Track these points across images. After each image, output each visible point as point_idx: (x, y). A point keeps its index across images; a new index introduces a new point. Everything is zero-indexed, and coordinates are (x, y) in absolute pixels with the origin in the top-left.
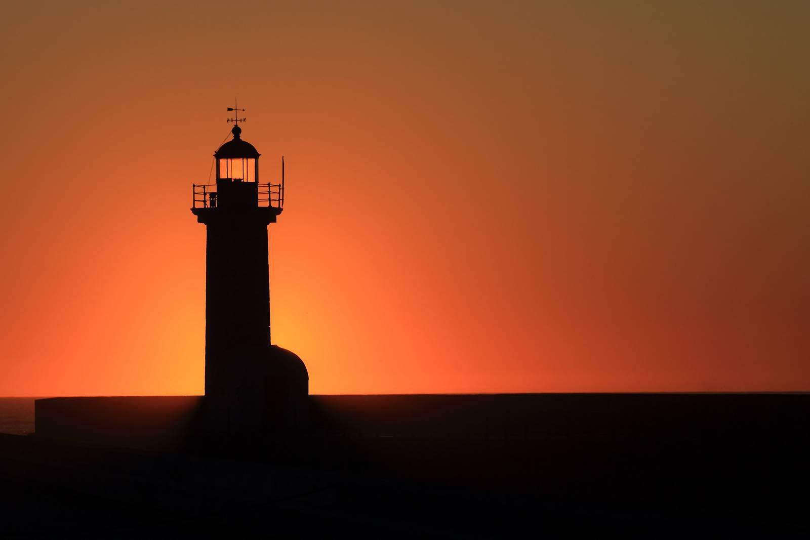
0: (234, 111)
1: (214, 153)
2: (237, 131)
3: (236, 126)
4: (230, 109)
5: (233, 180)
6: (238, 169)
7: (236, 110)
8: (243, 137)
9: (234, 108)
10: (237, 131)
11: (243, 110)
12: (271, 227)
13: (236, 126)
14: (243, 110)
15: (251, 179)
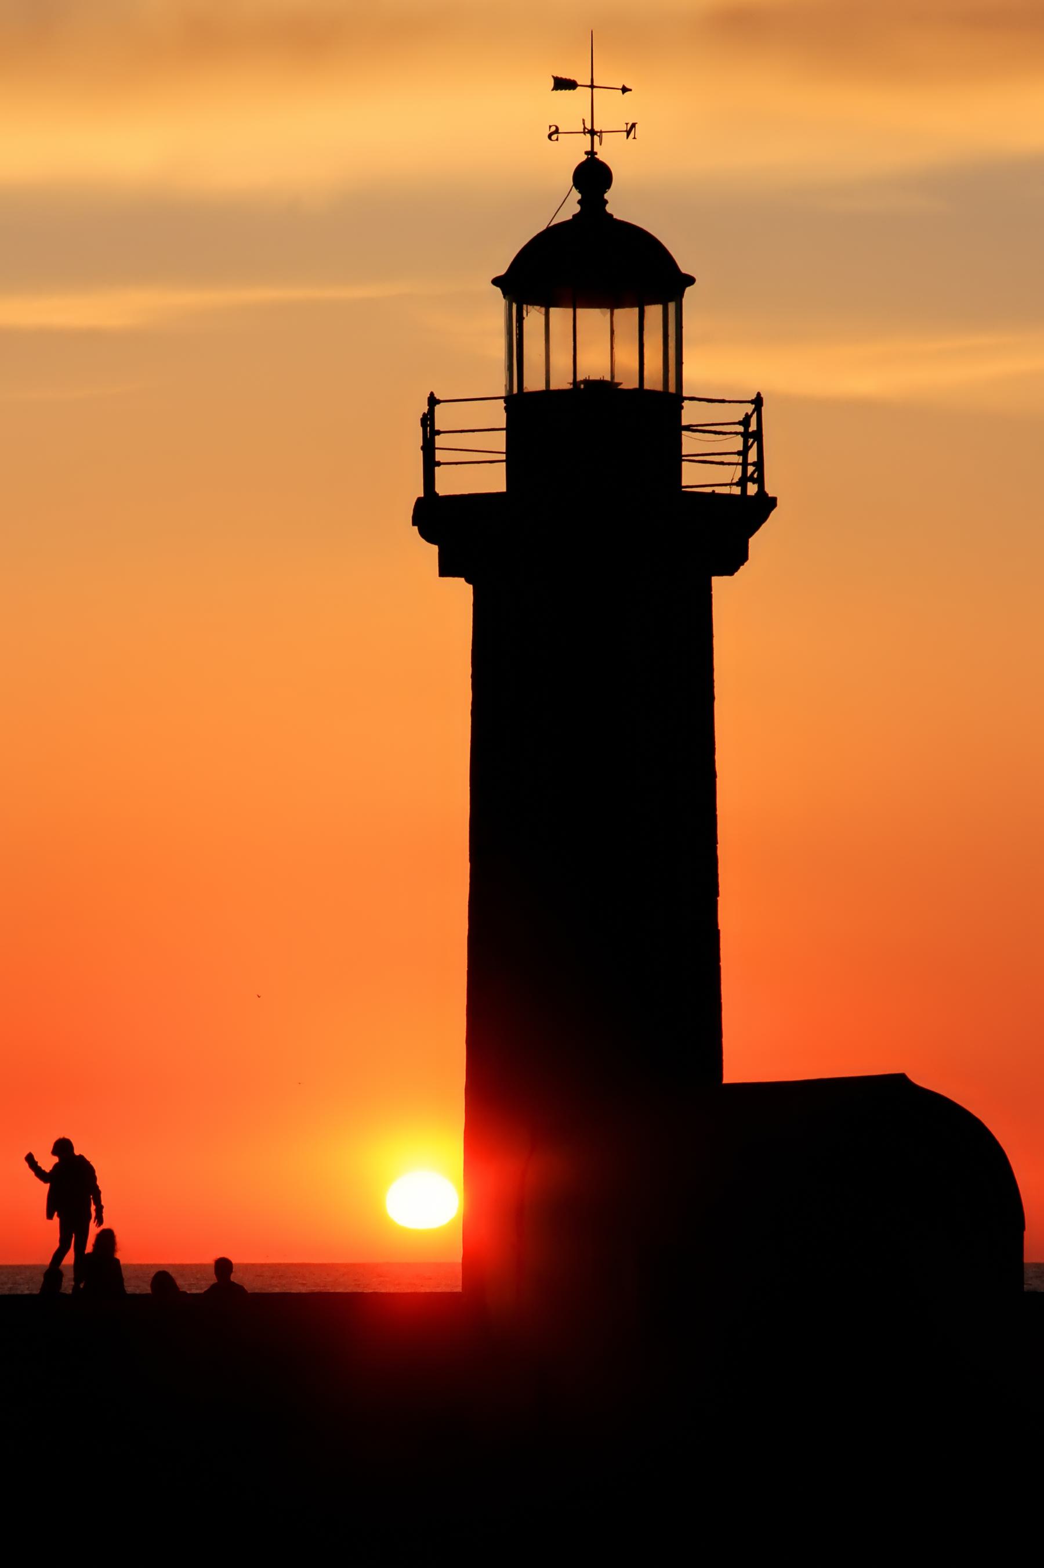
0: (582, 94)
1: (502, 271)
2: (592, 177)
3: (591, 153)
4: (562, 84)
5: (582, 386)
6: (592, 346)
7: (592, 86)
8: (619, 204)
9: (583, 79)
10: (592, 177)
11: (625, 90)
12: (717, 581)
13: (591, 153)
14: (625, 90)
15: (653, 380)
